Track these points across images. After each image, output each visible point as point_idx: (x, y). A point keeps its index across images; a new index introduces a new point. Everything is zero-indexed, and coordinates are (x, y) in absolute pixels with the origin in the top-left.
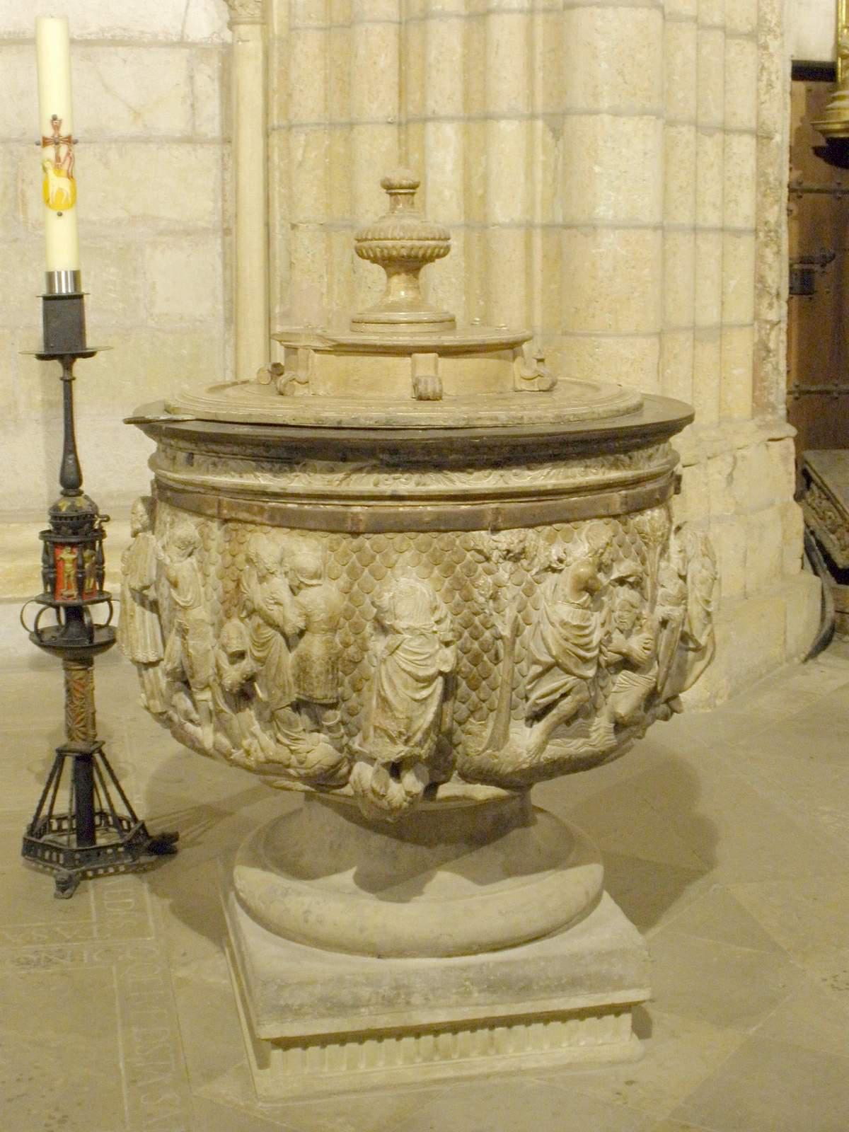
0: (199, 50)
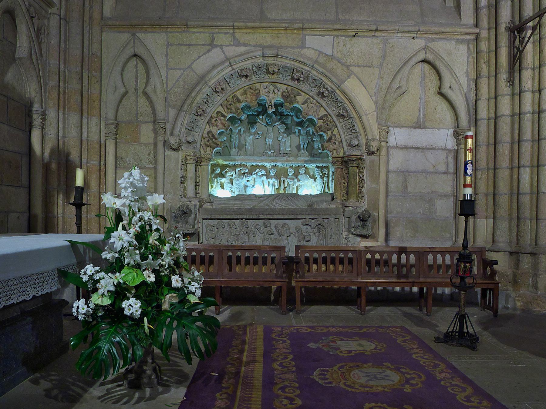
0: (449, 151)
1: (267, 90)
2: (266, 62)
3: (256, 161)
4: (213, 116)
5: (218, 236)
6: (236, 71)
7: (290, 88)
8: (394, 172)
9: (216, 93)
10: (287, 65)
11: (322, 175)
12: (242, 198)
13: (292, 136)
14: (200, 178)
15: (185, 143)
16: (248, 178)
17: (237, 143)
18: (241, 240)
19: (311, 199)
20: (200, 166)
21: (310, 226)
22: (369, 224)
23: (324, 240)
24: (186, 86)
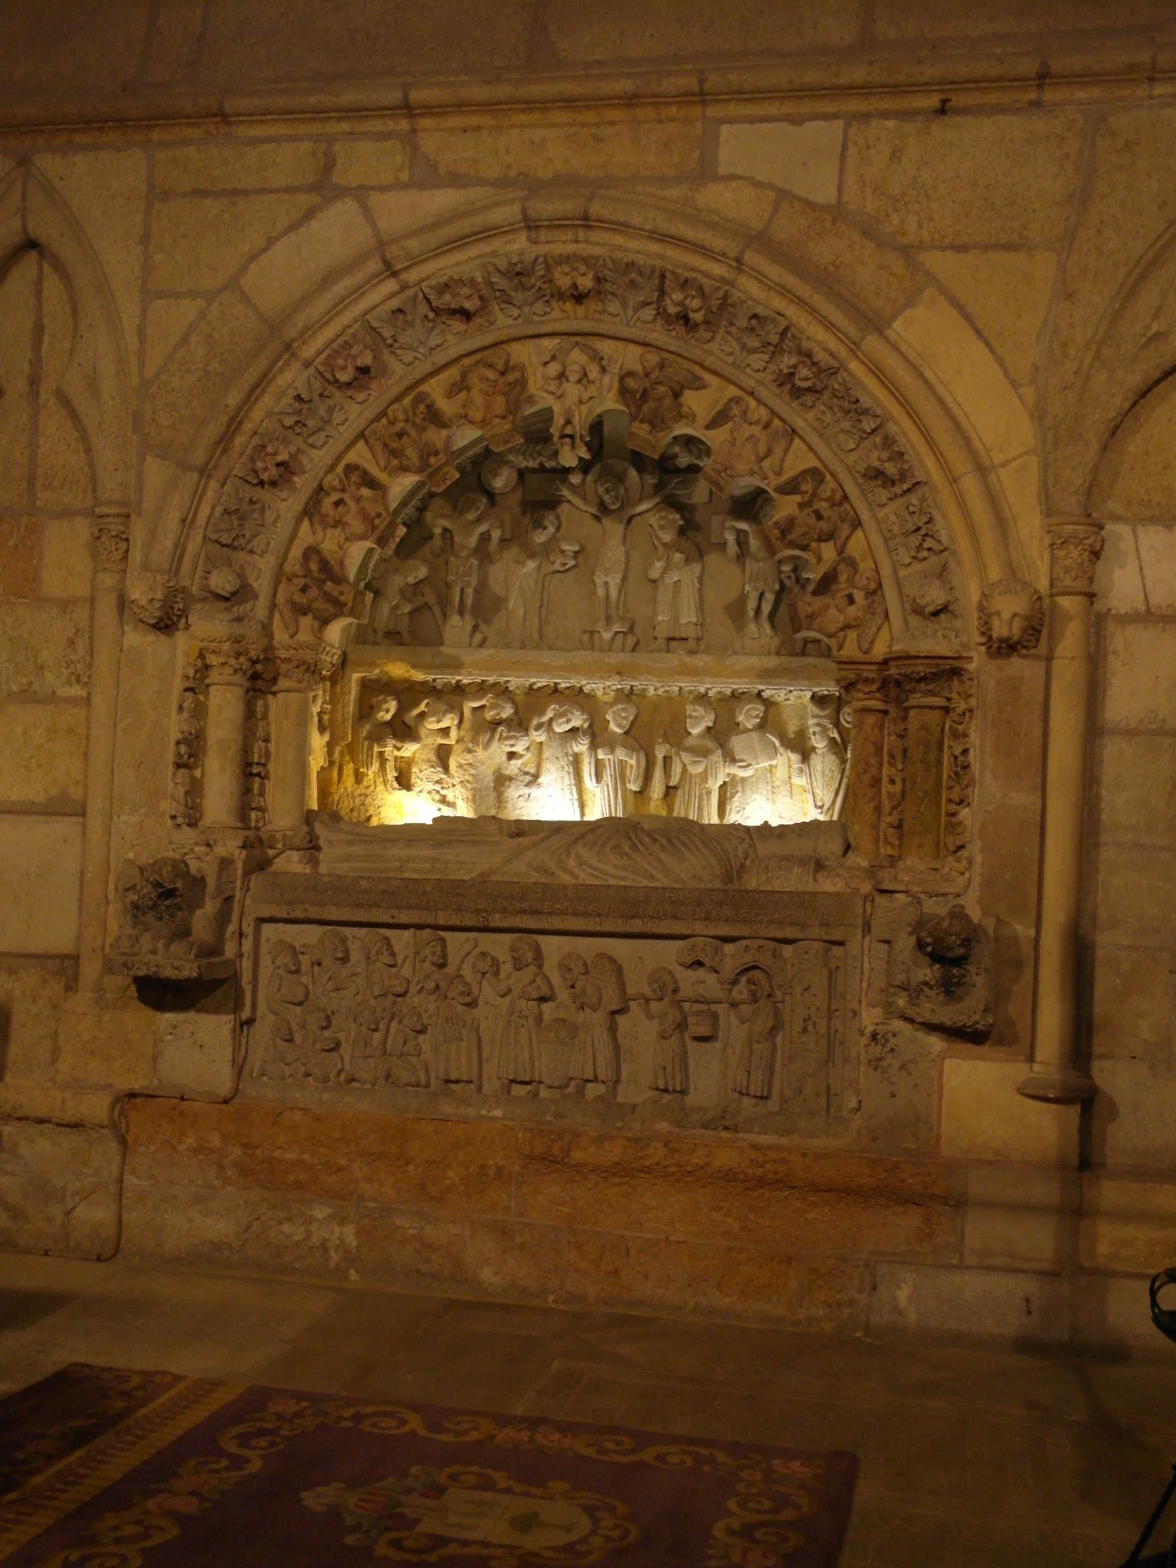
1: (554, 368)
2: (541, 249)
3: (545, 670)
4: (326, 484)
6: (415, 295)
7: (653, 359)
8: (1130, 733)
9: (340, 388)
10: (630, 257)
11: (836, 735)
13: (713, 559)
15: (204, 600)
16: (512, 742)
17: (470, 591)
19: (752, 846)
20: (274, 694)
21: (716, 972)
22: (979, 982)
24: (215, 366)
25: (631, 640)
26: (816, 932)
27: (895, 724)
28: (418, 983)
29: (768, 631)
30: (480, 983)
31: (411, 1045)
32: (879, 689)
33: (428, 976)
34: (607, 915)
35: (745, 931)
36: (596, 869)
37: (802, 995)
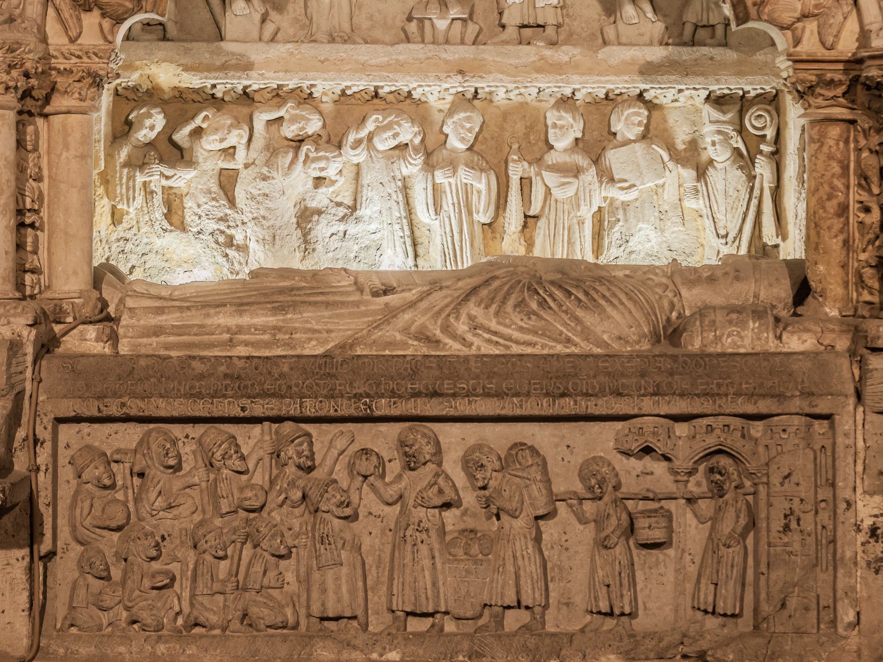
3: (363, 68)
5: (140, 519)
11: (741, 146)
12: (282, 291)
14: (45, 186)
16: (322, 164)
18: (273, 537)
19: (677, 294)
21: (667, 458)
23: (750, 541)
25: (472, 29)
26: (796, 404)
27: (866, 137)
28: (280, 492)
29: (650, 15)
30: (360, 489)
31: (271, 574)
32: (844, 94)
33: (292, 484)
34: (528, 394)
35: (706, 406)
36: (495, 333)
37: (782, 484)
